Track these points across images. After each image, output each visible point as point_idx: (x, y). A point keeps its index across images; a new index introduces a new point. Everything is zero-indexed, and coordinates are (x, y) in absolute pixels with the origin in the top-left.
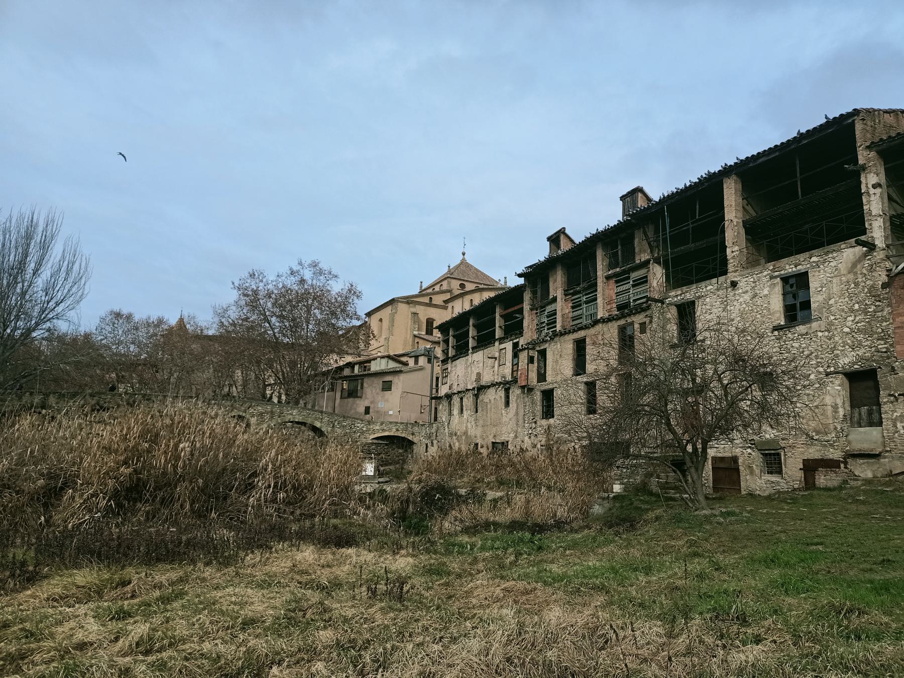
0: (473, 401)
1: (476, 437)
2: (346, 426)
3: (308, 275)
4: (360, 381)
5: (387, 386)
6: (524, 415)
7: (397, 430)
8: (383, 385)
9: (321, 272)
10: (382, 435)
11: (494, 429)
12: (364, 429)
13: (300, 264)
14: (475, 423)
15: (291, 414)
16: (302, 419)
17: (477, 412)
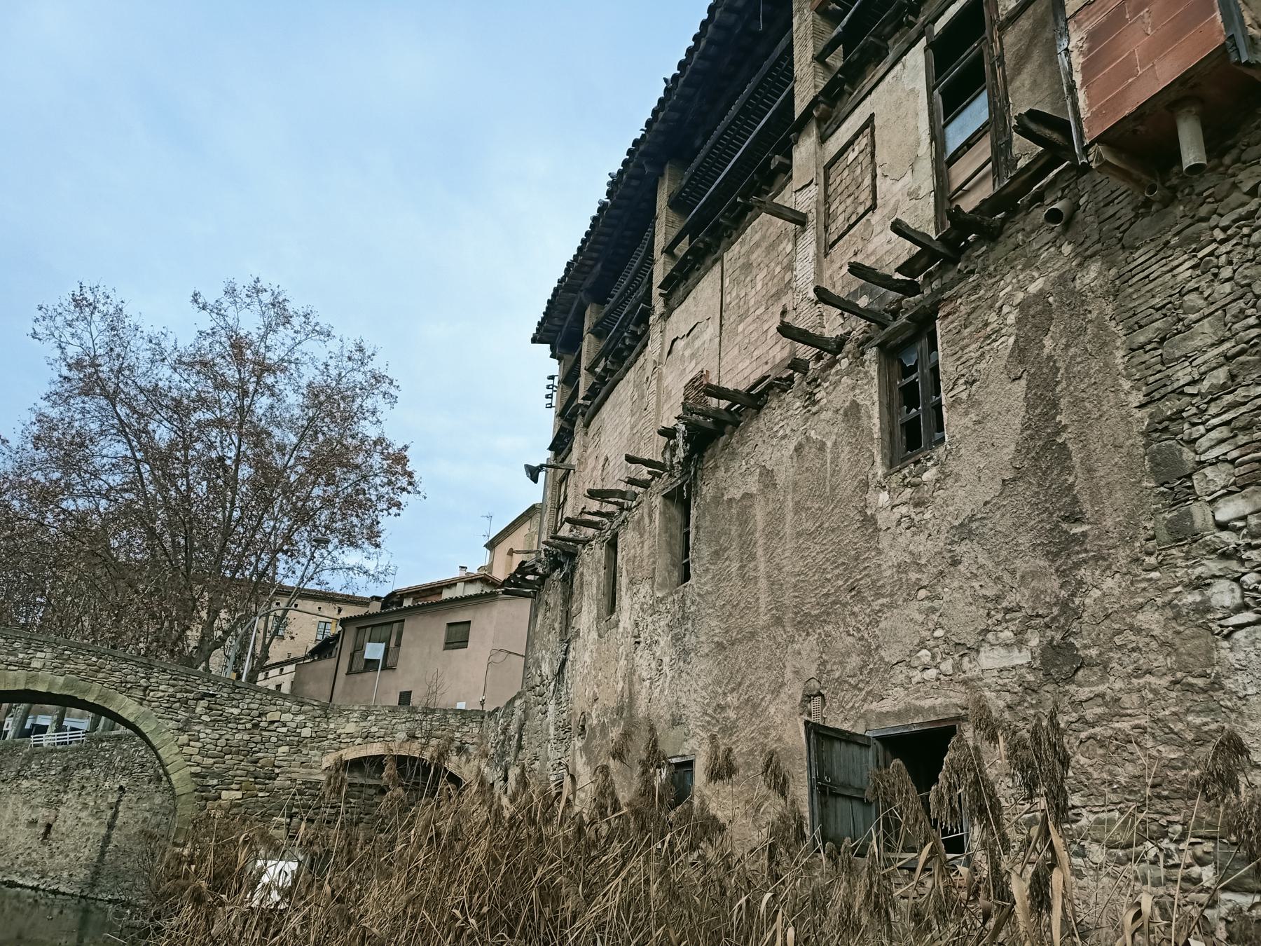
0: (666, 529)
1: (676, 722)
2: (237, 719)
3: (250, 323)
4: (396, 626)
5: (458, 638)
6: (1160, 428)
7: (412, 737)
8: (448, 635)
9: (280, 314)
10: (363, 753)
11: (808, 645)
12: (306, 732)
13: (231, 292)
14: (677, 639)
15: (23, 665)
16: (65, 685)
17: (686, 577)
